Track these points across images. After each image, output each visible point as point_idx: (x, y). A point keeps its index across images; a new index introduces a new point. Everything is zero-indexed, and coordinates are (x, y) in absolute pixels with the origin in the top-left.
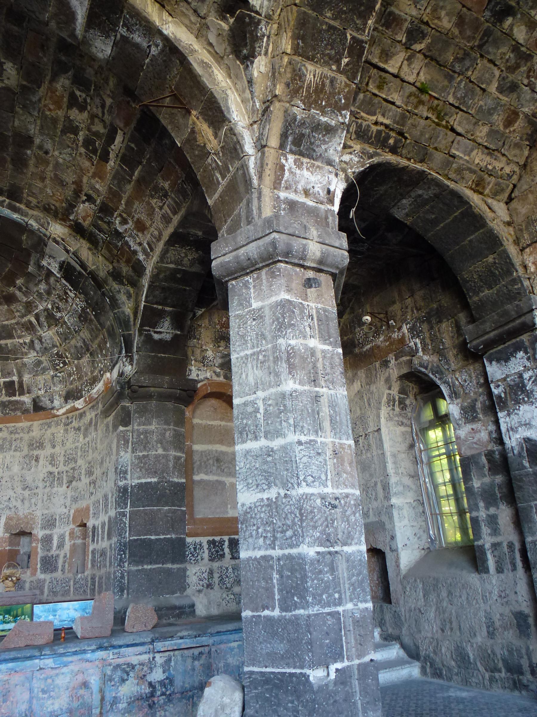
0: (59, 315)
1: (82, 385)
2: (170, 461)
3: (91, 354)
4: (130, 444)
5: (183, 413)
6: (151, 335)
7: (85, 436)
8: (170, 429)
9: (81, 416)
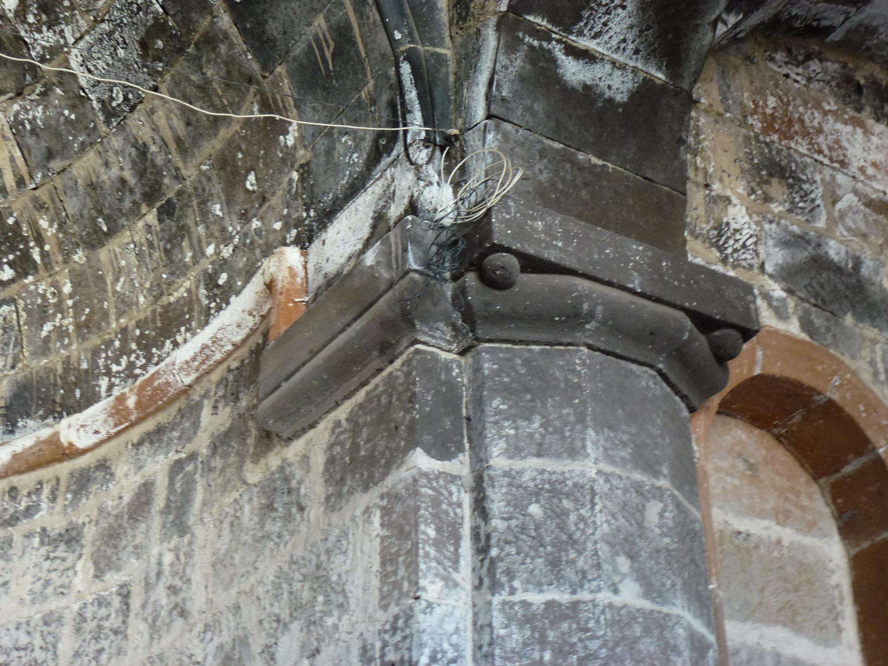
0: (47, 38)
1: (95, 353)
2: (676, 650)
3: (167, 211)
4: (466, 547)
5: (683, 437)
6: (553, 61)
7: (102, 566)
8: (658, 493)
9: (82, 483)
